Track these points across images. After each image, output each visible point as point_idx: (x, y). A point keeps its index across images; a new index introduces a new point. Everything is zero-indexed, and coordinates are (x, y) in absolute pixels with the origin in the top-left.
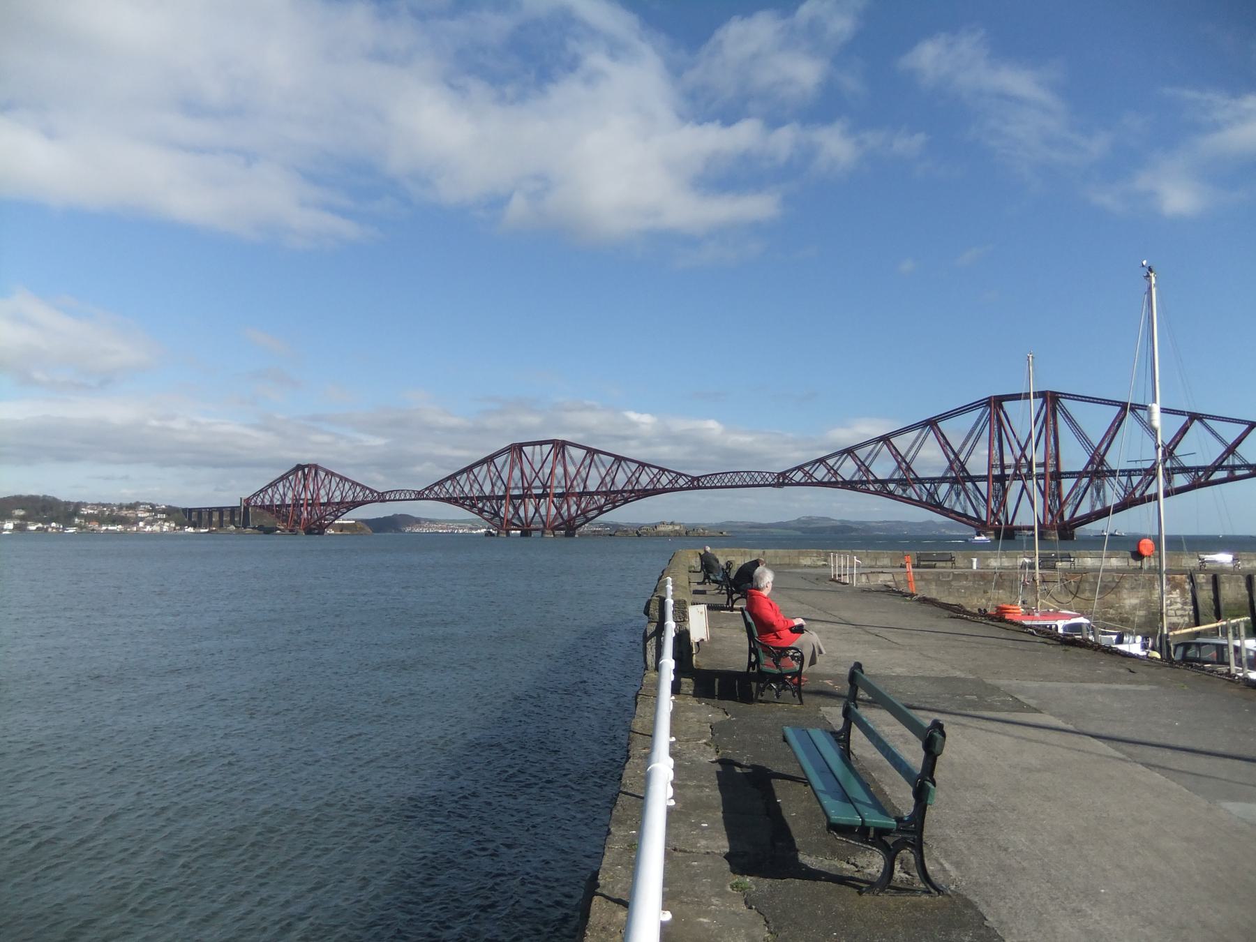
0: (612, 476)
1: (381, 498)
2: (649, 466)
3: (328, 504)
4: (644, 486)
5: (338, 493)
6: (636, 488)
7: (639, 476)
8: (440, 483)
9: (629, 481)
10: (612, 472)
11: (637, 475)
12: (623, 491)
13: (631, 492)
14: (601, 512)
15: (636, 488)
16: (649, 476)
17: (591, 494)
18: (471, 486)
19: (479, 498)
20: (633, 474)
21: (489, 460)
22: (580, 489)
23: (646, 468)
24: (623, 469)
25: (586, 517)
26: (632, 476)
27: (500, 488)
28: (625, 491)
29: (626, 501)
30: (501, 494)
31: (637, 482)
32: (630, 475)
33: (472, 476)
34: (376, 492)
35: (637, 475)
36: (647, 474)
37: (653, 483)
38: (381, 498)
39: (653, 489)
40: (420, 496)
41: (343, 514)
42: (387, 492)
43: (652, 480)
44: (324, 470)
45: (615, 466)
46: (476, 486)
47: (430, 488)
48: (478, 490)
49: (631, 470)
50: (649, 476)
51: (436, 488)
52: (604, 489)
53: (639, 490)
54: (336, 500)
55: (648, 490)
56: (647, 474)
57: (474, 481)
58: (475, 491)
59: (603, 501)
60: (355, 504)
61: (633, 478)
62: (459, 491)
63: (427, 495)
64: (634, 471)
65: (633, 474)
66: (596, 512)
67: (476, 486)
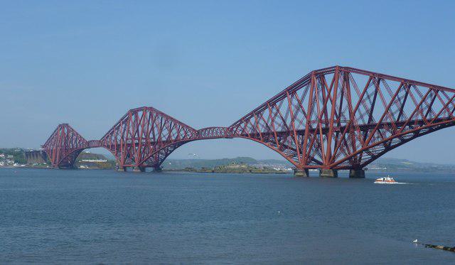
0: (399, 104)
1: (199, 135)
2: (443, 89)
3: (159, 142)
4: (437, 113)
5: (165, 132)
6: (428, 117)
7: (432, 103)
8: (246, 119)
9: (418, 109)
10: (399, 99)
11: (429, 101)
12: (410, 123)
13: (421, 122)
14: (388, 148)
15: (428, 117)
16: (442, 102)
17: (375, 125)
18: (273, 121)
19: (280, 134)
20: (424, 100)
21: (292, 90)
22: (363, 120)
23: (440, 93)
24: (411, 96)
25: (369, 153)
26: (421, 103)
27: (301, 122)
28: (413, 122)
29: (417, 134)
30: (302, 128)
31: (430, 110)
32: (419, 100)
33: (274, 111)
34: (194, 130)
35: (429, 101)
36: (440, 99)
37: (448, 110)
38: (199, 135)
39: (449, 119)
40: (230, 133)
41: (171, 152)
42: (202, 130)
43: (446, 107)
44: (155, 110)
45: (402, 93)
46: (278, 120)
47: (237, 124)
48: (280, 125)
49: (421, 96)
50: (442, 102)
51: (243, 125)
52: (389, 121)
53: (429, 121)
54: (164, 139)
55: (440, 120)
56: (440, 99)
57: (276, 115)
58: (276, 126)
59: (388, 135)
60: (179, 143)
61: (424, 105)
62: (263, 126)
63: (235, 132)
64: (424, 95)
65: (424, 100)
66: (381, 148)
67: (278, 120)
